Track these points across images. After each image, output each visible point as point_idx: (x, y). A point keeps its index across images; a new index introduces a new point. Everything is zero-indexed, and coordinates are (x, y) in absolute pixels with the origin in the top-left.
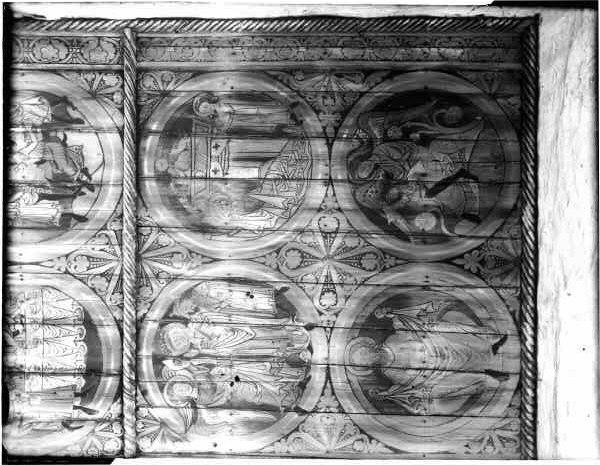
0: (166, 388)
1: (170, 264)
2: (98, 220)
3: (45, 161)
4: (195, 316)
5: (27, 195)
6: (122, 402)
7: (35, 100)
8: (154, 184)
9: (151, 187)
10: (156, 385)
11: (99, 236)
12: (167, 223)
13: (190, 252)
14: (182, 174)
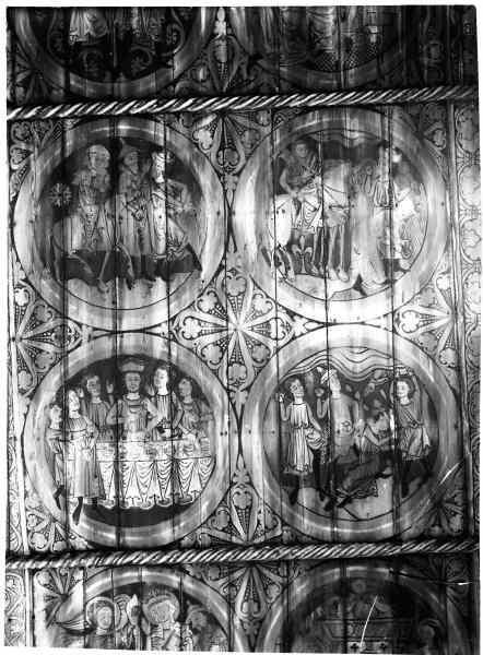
1: (246, 600)
2: (292, 517)
3: (358, 455)
4: (189, 631)
5: (317, 436)
7: (427, 442)
8: (337, 577)
9: (335, 574)
10: (110, 587)
12: (293, 594)
13: (261, 621)
14: (349, 609)
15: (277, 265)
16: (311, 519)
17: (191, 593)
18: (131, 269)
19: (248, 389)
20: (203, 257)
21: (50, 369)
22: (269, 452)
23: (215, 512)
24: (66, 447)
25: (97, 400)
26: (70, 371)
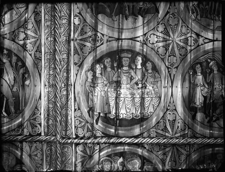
0: (109, 158)
1: (170, 160)
2: (193, 125)
5: (206, 90)
6: (102, 137)
8: (210, 152)
11: (185, 126)
12: (191, 159)
15: (193, 13)
16: (201, 127)
17: (147, 157)
18: (128, 11)
19: (177, 68)
20: (160, 7)
21: (89, 54)
22: (184, 96)
23: (159, 121)
24: (95, 90)
25: (109, 69)
26: (97, 56)
